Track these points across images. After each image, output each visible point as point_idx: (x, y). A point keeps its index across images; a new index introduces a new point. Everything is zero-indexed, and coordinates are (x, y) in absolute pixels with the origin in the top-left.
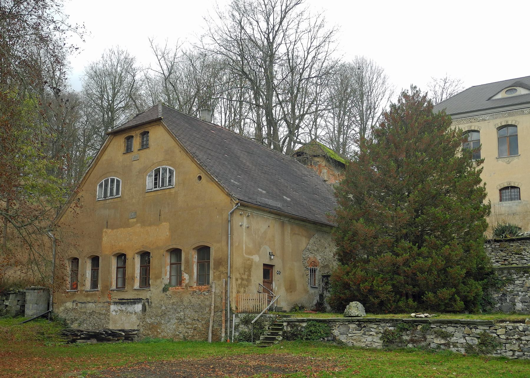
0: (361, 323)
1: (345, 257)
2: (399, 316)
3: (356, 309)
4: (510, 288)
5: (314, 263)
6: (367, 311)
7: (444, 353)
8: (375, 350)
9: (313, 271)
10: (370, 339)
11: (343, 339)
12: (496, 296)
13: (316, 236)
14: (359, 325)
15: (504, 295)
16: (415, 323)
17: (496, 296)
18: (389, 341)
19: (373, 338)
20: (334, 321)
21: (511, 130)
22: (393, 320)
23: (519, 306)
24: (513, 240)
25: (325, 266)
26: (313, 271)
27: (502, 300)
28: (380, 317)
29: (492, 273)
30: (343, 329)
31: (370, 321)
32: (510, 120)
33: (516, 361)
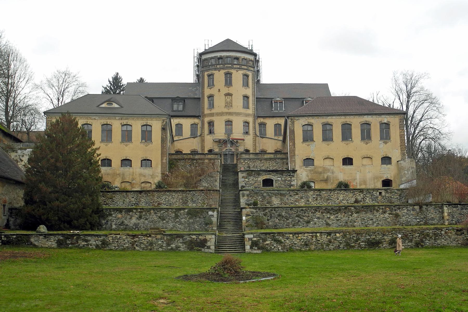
0: (46, 236)
1: (29, 200)
2: (65, 232)
3: (43, 229)
4: (110, 218)
5: (5, 202)
6: (48, 230)
7: (86, 248)
8: (53, 248)
9: (4, 206)
10: (50, 243)
11: (36, 243)
12: (103, 222)
13: (6, 186)
14: (45, 237)
15: (107, 221)
16: (73, 235)
17: (103, 222)
18: (60, 244)
19: (52, 242)
20: (32, 235)
21: (109, 126)
22: (62, 234)
23: (114, 227)
24: (109, 192)
25: (10, 203)
26: (4, 206)
27: (106, 224)
28: (55, 232)
29: (102, 211)
30: (36, 239)
31: (51, 235)
32: (109, 122)
33: (116, 250)
